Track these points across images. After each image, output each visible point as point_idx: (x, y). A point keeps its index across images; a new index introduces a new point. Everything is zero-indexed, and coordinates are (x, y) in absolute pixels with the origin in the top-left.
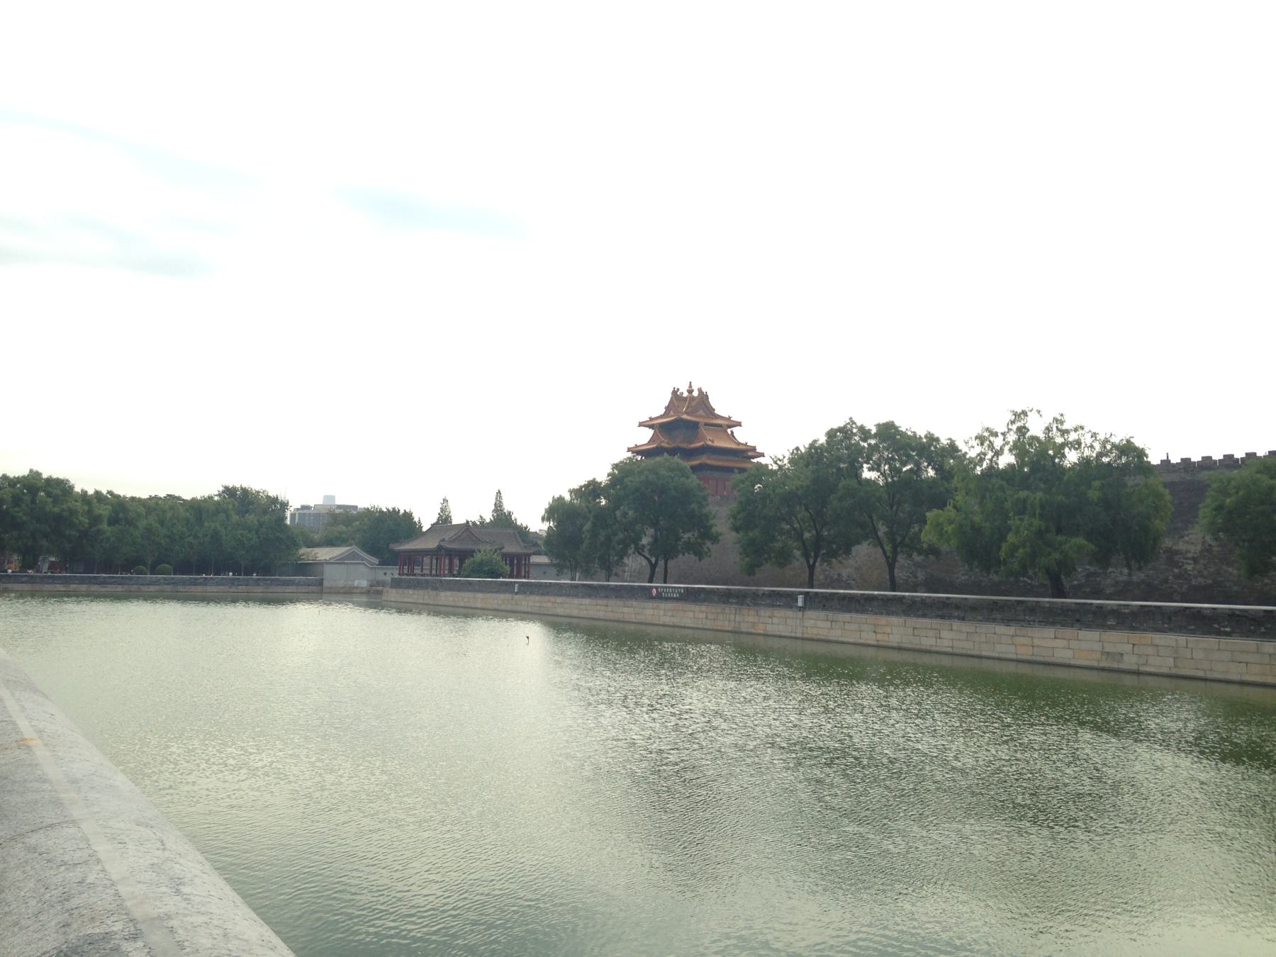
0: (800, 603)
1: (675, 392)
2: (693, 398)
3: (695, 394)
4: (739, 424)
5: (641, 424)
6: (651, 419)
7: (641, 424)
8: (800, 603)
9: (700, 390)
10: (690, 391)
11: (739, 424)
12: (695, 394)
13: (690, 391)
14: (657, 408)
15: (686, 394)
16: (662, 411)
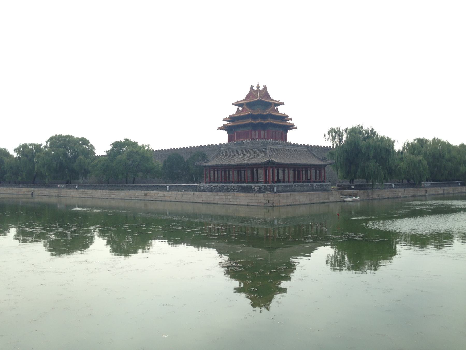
0: (168, 189)
1: (252, 87)
2: (260, 91)
3: (261, 88)
4: (283, 104)
5: (233, 104)
6: (237, 102)
7: (233, 104)
8: (168, 189)
9: (265, 87)
10: (258, 87)
11: (283, 104)
12: (261, 88)
13: (258, 87)
14: (242, 95)
15: (255, 88)
16: (244, 97)
